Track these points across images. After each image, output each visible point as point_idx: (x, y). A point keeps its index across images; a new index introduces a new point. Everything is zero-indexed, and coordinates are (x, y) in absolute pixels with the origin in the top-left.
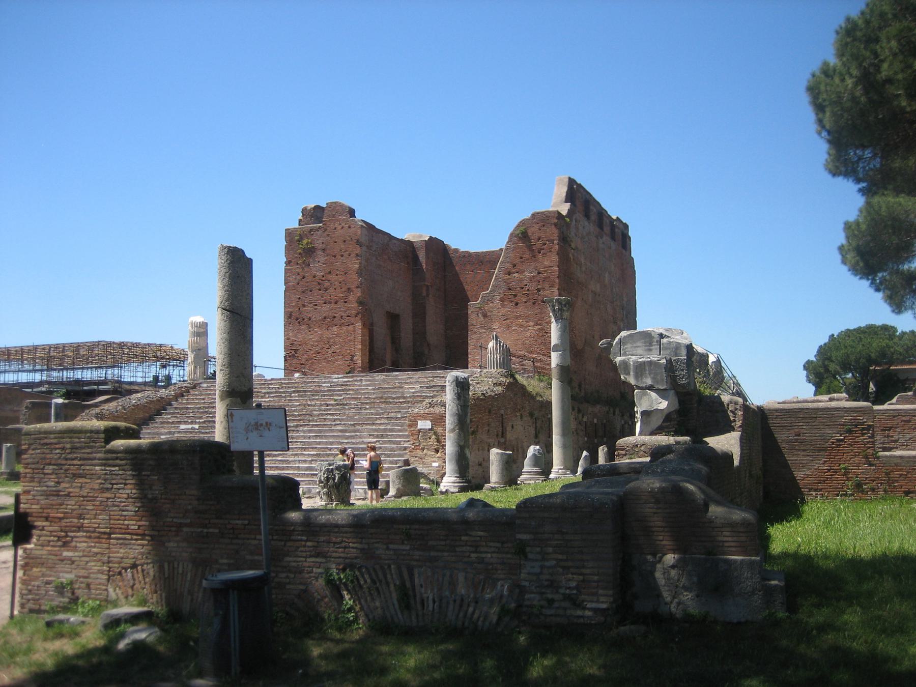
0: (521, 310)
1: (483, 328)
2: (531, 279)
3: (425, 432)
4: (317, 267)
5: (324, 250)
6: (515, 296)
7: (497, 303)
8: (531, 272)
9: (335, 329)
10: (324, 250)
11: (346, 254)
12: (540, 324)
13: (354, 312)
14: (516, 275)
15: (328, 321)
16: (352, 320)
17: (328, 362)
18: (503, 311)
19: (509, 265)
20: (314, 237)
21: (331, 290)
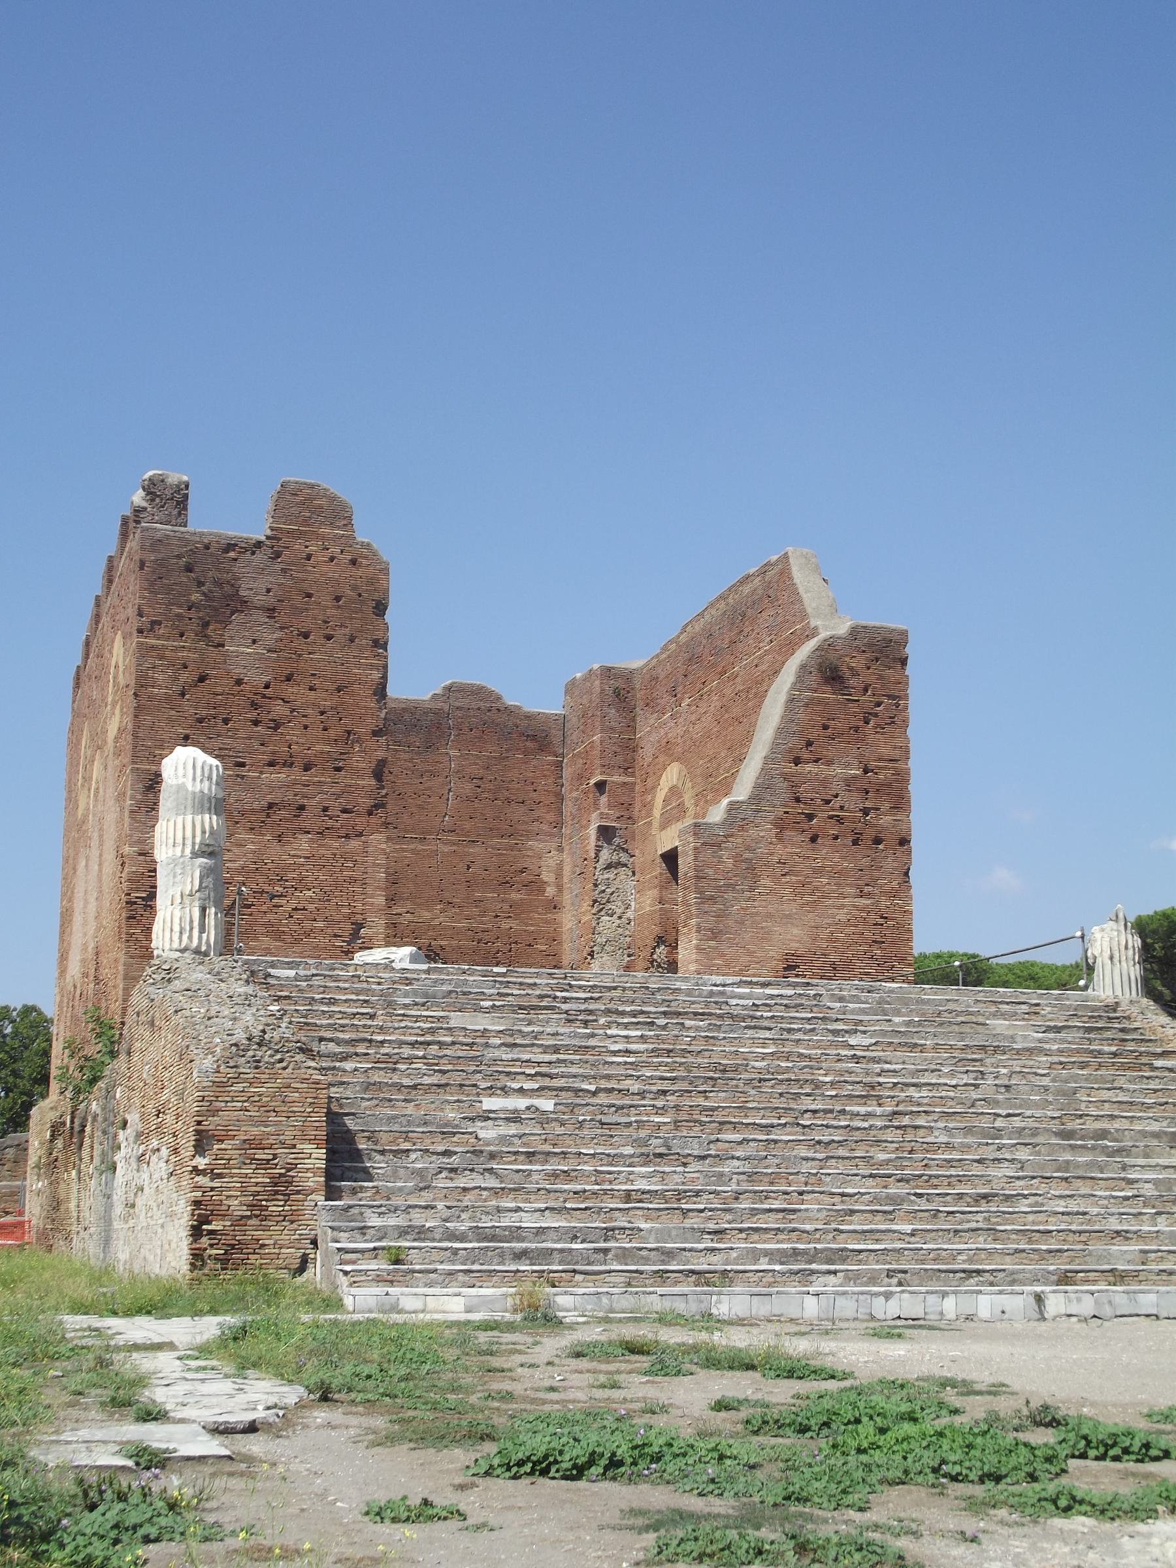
0: (828, 855)
1: (732, 887)
2: (849, 782)
4: (246, 652)
5: (271, 611)
6: (810, 817)
7: (766, 830)
8: (847, 765)
9: (303, 844)
10: (271, 611)
11: (341, 634)
12: (869, 895)
13: (366, 802)
14: (809, 767)
16: (360, 822)
17: (278, 935)
18: (780, 851)
19: (795, 742)
20: (237, 568)
21: (292, 732)
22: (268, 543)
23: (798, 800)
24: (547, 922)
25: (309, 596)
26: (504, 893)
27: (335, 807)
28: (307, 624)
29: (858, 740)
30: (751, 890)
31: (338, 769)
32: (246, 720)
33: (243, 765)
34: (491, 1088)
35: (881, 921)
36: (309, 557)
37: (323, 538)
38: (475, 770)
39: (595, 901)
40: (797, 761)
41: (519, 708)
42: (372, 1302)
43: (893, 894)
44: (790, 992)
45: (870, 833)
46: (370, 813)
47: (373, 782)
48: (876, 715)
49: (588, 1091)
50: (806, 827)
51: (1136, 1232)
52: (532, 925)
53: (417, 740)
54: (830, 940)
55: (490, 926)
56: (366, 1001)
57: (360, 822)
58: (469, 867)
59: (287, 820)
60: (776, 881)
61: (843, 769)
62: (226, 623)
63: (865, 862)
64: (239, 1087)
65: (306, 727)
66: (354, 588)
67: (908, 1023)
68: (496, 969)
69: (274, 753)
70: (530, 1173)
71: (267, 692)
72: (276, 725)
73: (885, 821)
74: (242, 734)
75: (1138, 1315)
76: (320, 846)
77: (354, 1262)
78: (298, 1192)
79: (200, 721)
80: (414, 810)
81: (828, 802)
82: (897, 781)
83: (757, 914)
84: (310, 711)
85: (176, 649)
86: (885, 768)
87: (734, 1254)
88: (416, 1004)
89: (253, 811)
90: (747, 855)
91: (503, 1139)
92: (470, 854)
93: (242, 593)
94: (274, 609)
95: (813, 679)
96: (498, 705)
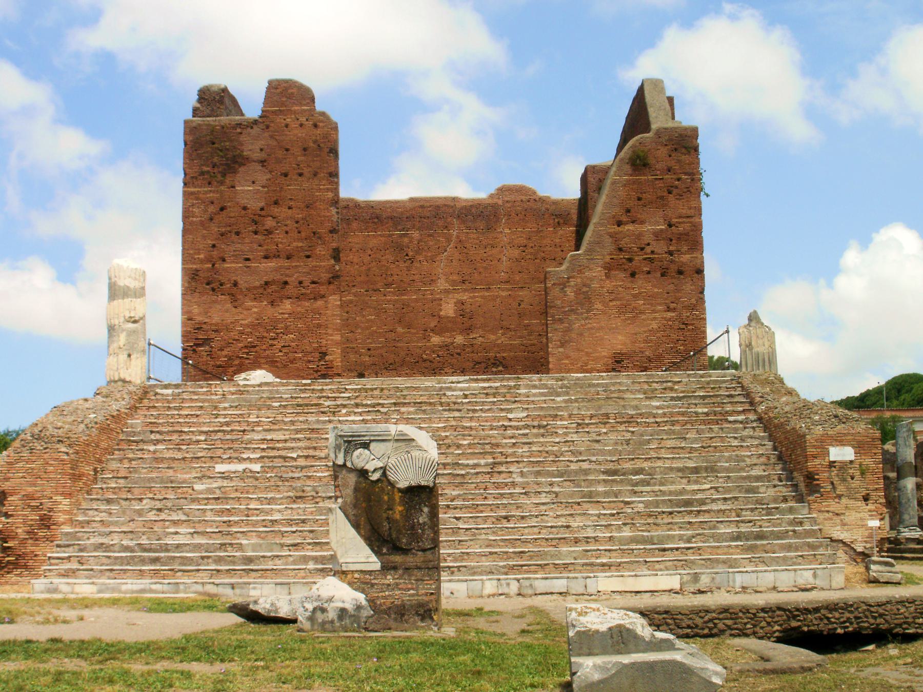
0: (643, 285)
2: (657, 235)
3: (844, 466)
4: (248, 189)
5: (263, 162)
7: (597, 272)
8: (658, 223)
9: (287, 305)
10: (263, 162)
12: (674, 310)
13: (325, 276)
14: (630, 227)
15: (274, 290)
16: (323, 289)
18: (608, 284)
19: (617, 210)
20: (242, 138)
21: (279, 236)
22: (260, 120)
23: (620, 250)
25: (287, 150)
27: (307, 280)
28: (286, 168)
29: (663, 205)
30: (588, 311)
31: (308, 257)
32: (249, 231)
33: (248, 259)
34: (230, 458)
35: (684, 326)
36: (287, 126)
37: (295, 112)
38: (523, 241)
40: (619, 224)
41: (549, 197)
42: (42, 587)
43: (693, 307)
44: (498, 384)
45: (674, 268)
46: (330, 283)
47: (332, 262)
48: (676, 187)
49: (292, 458)
50: (626, 267)
51: (594, 538)
53: (481, 225)
54: (646, 341)
55: (535, 342)
56: (201, 407)
57: (323, 289)
58: (520, 305)
59: (276, 292)
60: (605, 304)
61: (653, 225)
62: (235, 172)
63: (671, 287)
64: (21, 465)
65: (287, 232)
66: (315, 142)
67: (566, 401)
68: (304, 382)
69: (267, 250)
70: (204, 510)
71: (263, 213)
72: (269, 232)
73: (686, 258)
74: (247, 240)
75: (552, 593)
76: (298, 306)
77: (57, 565)
78: (54, 524)
79: (222, 235)
80: (481, 270)
81: (642, 249)
82: (692, 230)
83: (591, 328)
84: (289, 222)
85: (206, 193)
86: (684, 223)
87: (291, 559)
88: (232, 407)
89: (255, 288)
90: (585, 289)
91: (209, 491)
92: (519, 296)
93: (245, 153)
94: (265, 161)
95: (628, 168)
96: (534, 197)
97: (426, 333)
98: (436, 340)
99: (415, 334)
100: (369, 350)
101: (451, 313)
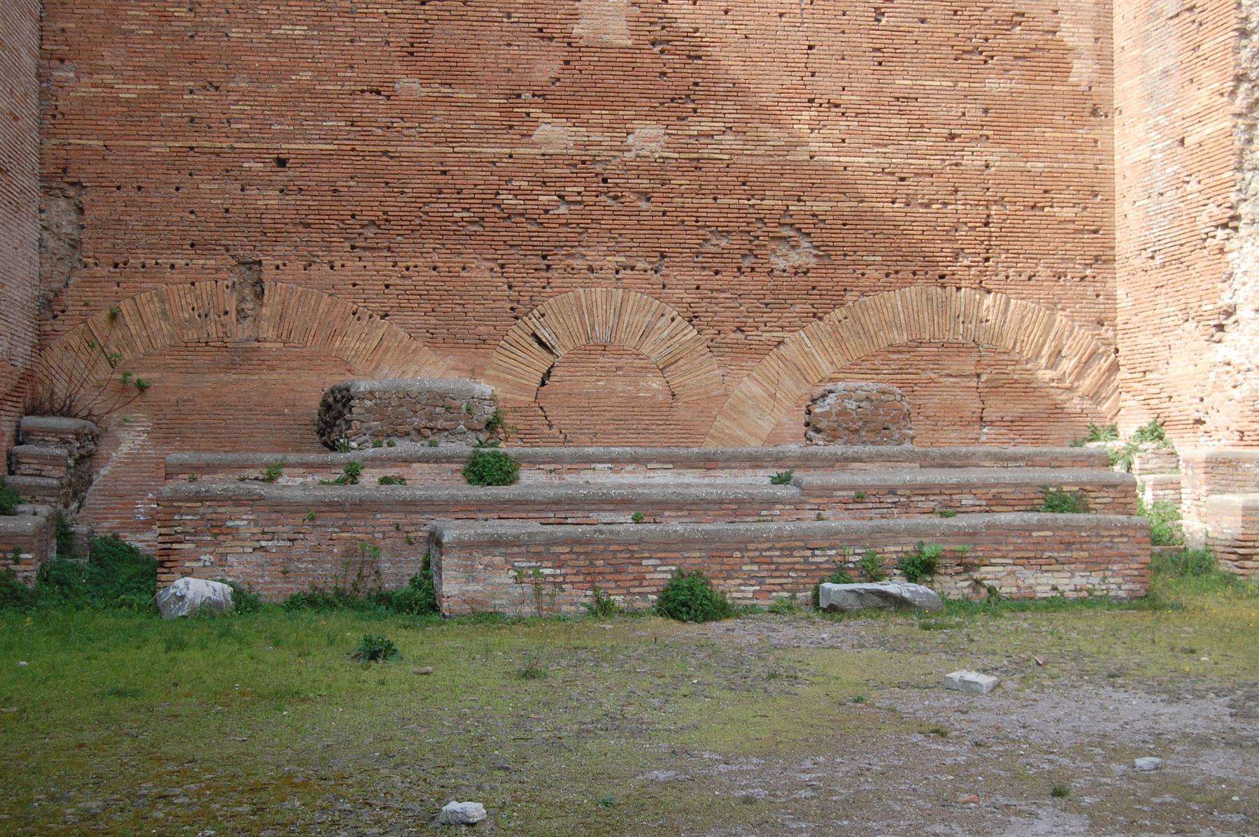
24: (1075, 147)
26: (969, 78)
39: (1239, 79)
52: (1038, 156)
97: (514, 110)
98: (554, 134)
99: (471, 105)
100: (282, 162)
101: (618, 33)
